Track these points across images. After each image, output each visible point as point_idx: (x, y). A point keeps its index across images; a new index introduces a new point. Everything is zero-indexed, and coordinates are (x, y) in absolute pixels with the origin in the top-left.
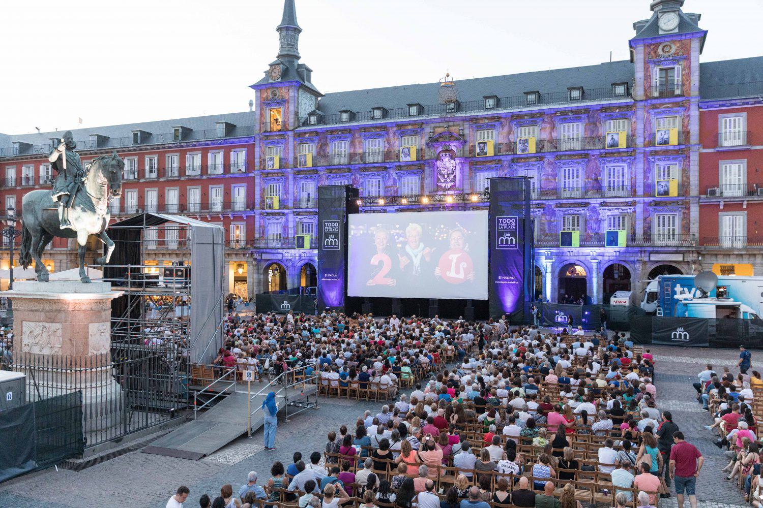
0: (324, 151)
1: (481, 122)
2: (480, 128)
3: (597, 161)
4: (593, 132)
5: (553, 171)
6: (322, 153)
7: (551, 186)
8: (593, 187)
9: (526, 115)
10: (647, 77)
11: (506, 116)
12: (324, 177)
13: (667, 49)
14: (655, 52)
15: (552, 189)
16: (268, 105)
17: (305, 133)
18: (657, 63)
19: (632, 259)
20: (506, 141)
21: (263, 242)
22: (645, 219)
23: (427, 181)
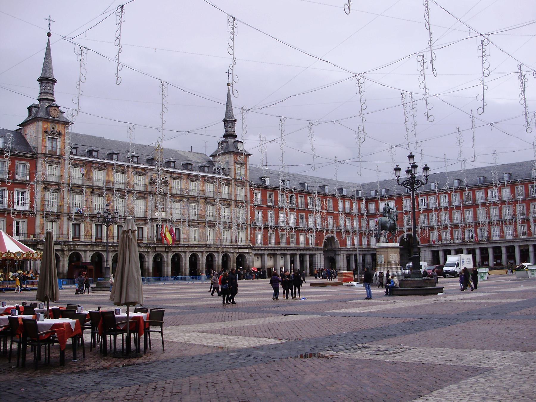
0: (89, 175)
1: (175, 175)
2: (175, 178)
6: (87, 176)
9: (194, 176)
10: (235, 169)
11: (185, 175)
16: (49, 133)
18: (238, 163)
23: (150, 204)
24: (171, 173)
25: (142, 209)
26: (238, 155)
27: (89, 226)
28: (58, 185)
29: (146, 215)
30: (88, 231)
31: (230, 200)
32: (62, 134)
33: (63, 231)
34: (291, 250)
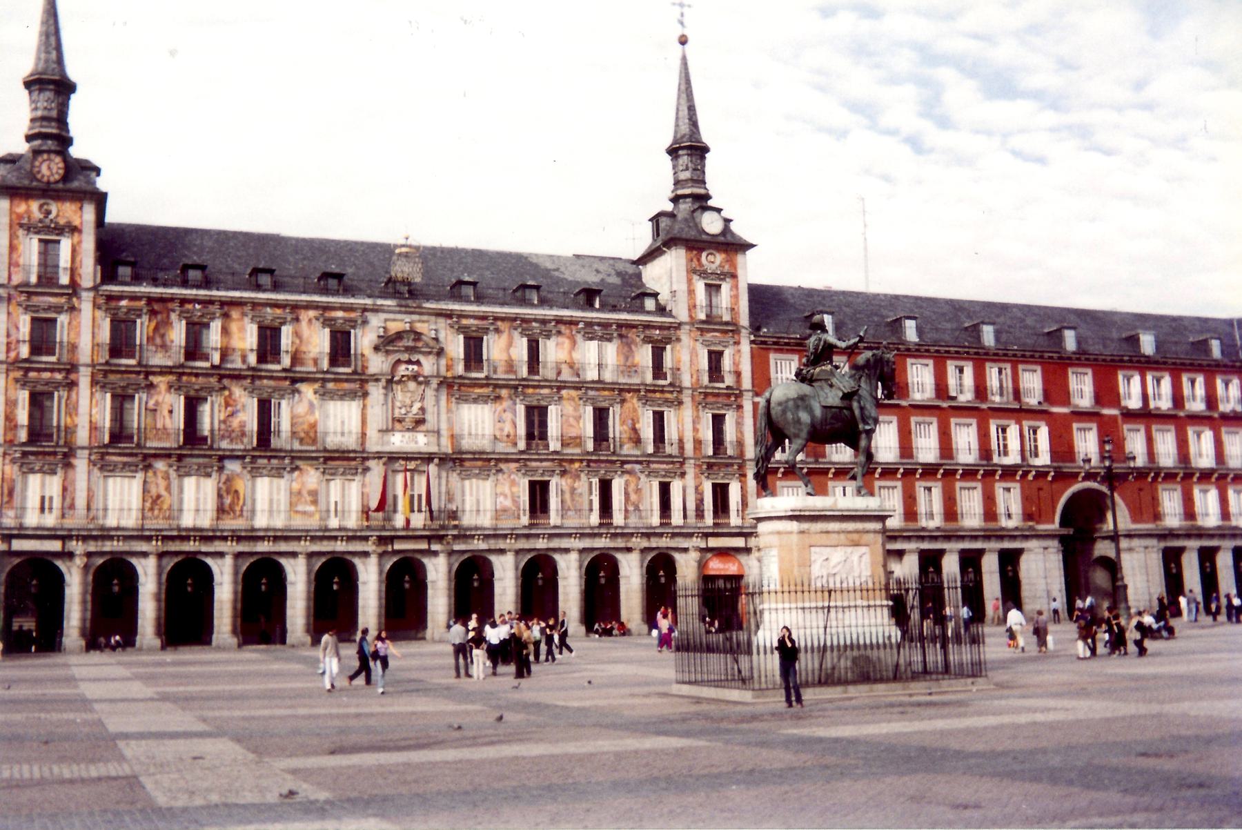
0: (163, 336)
1: (465, 322)
3: (635, 400)
4: (627, 358)
5: (576, 409)
7: (573, 432)
8: (630, 439)
9: (535, 320)
10: (691, 292)
11: (503, 319)
12: (163, 387)
13: (711, 258)
14: (699, 260)
15: (576, 438)
17: (120, 298)
18: (703, 274)
19: (685, 545)
20: (504, 357)
21: (11, 513)
22: (697, 488)
24: (448, 315)
25: (354, 425)
26: (701, 250)
27: (162, 483)
28: (59, 371)
29: (363, 444)
30: (159, 497)
31: (677, 387)
32: (74, 230)
33: (73, 499)
34: (922, 538)
